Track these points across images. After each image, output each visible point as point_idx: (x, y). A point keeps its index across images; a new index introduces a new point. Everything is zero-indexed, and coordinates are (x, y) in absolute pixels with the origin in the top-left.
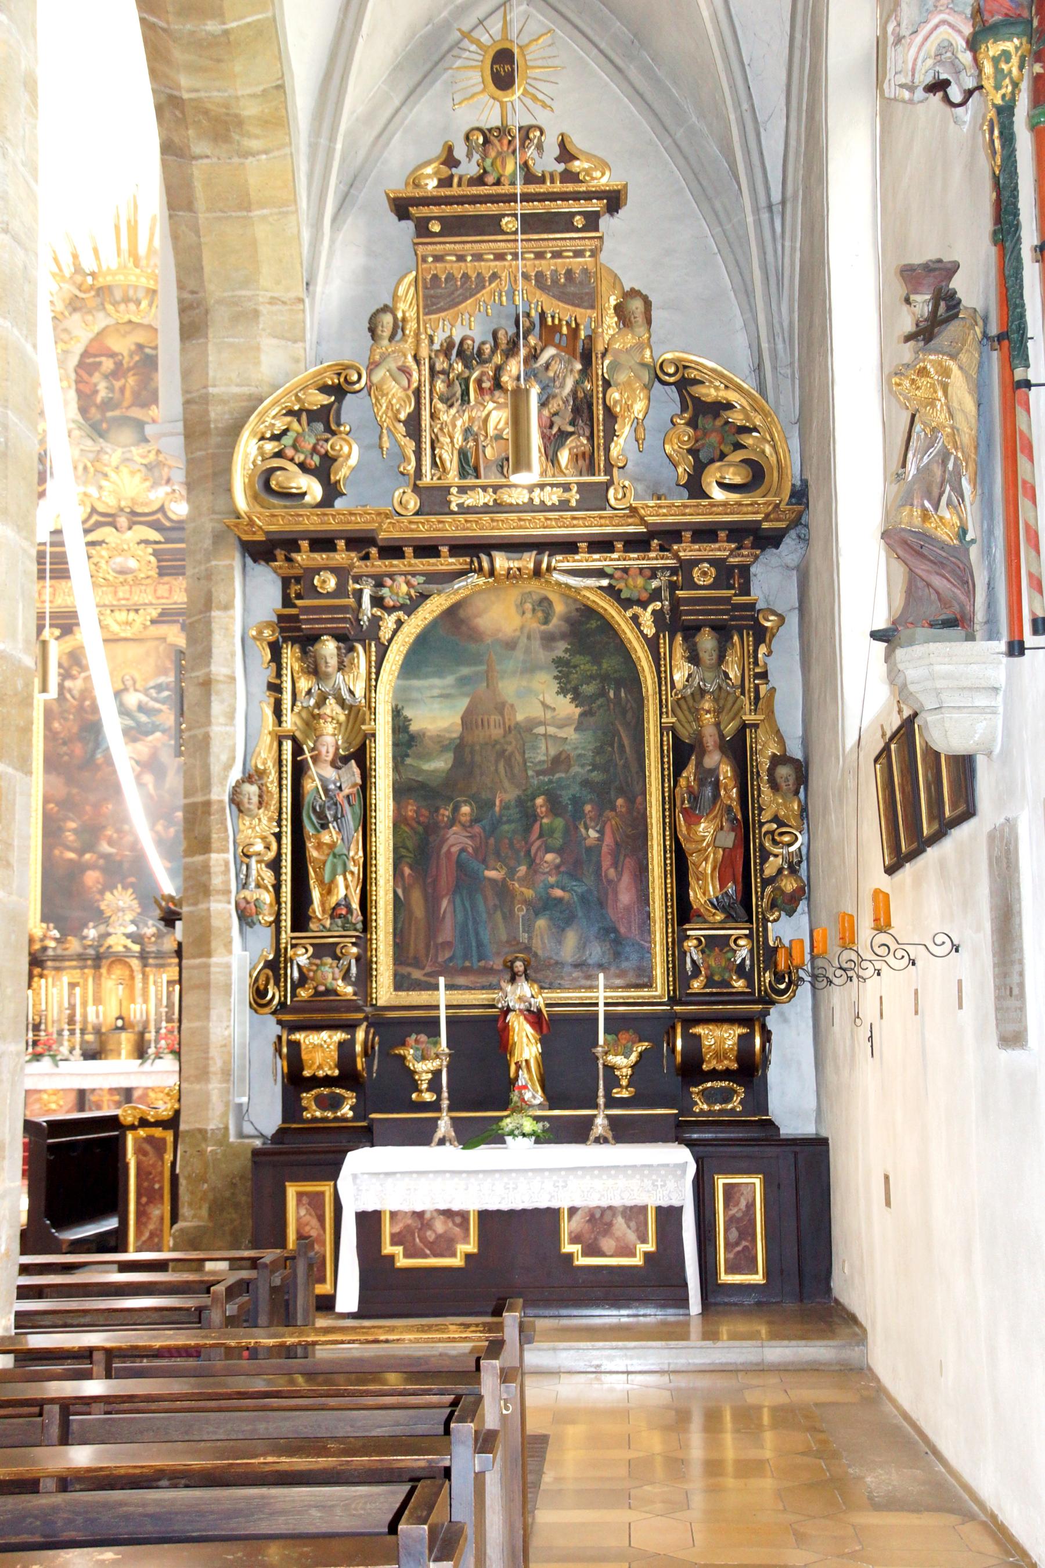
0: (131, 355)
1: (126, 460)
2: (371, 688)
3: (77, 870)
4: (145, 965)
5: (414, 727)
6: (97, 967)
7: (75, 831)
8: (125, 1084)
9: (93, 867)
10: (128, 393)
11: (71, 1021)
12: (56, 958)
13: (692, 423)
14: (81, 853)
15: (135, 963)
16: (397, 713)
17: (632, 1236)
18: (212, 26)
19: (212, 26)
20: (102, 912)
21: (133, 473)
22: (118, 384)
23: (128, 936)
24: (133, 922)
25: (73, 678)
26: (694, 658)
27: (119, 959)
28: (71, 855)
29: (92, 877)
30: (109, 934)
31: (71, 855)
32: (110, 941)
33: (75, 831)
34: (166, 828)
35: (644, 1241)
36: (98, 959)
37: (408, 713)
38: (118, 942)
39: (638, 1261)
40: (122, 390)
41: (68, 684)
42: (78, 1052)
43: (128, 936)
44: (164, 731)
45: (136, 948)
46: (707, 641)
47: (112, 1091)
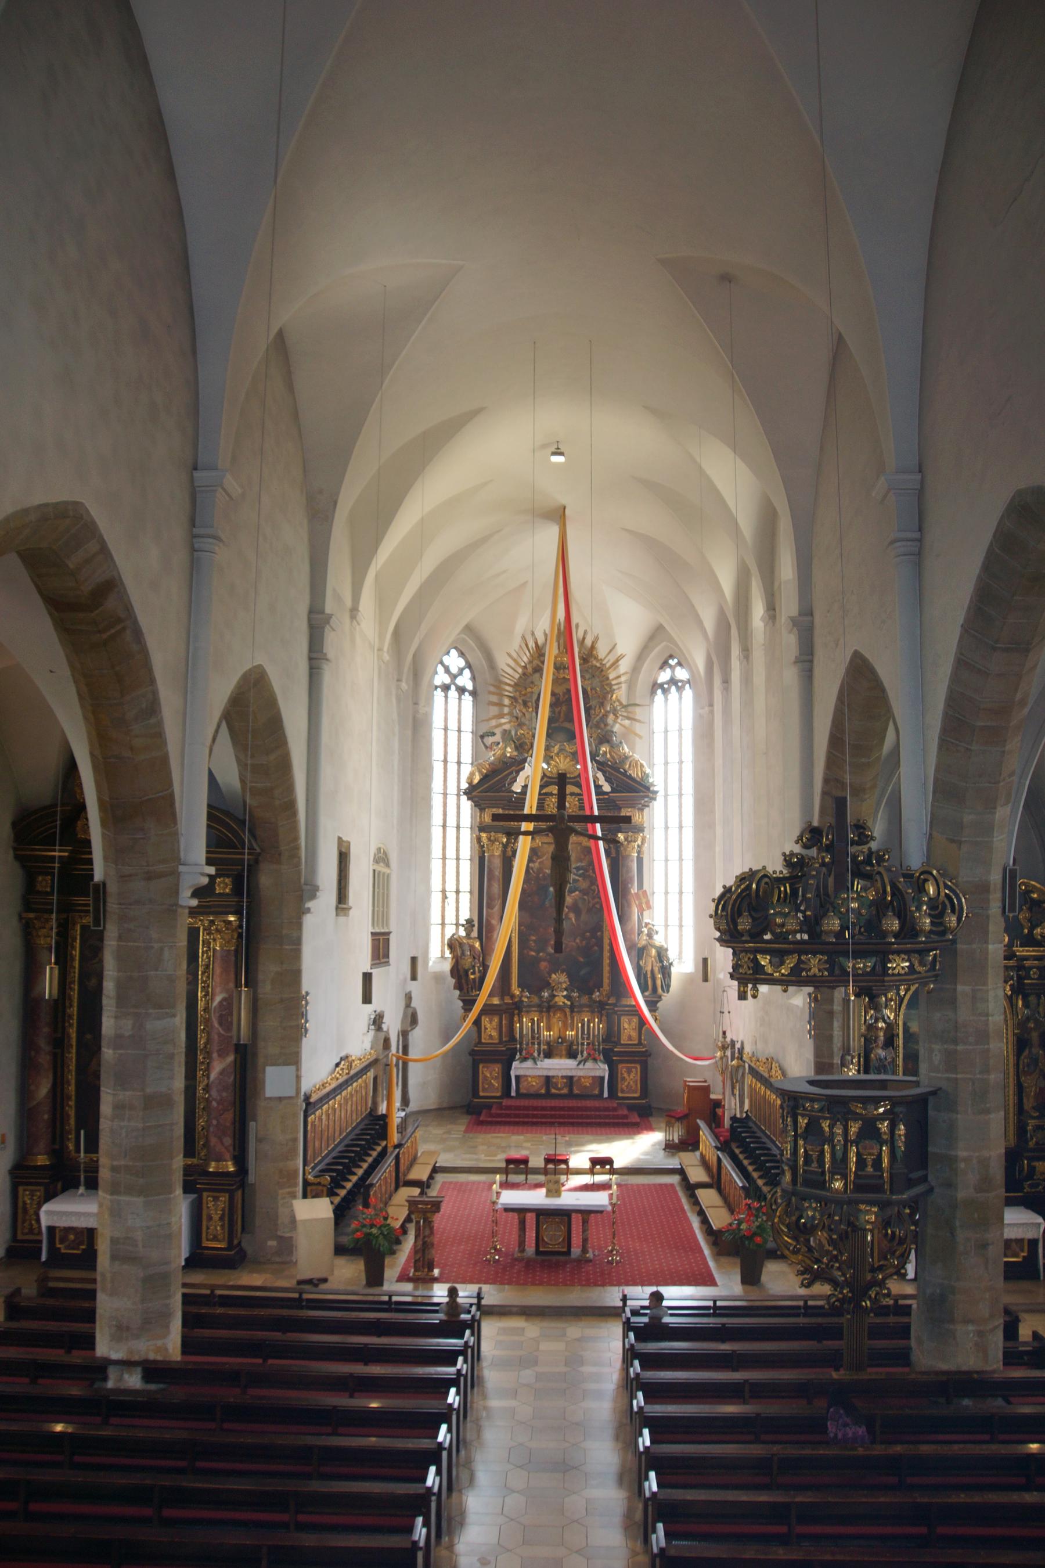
0: (564, 694)
1: (561, 750)
2: (897, 1016)
3: (537, 961)
4: (572, 1012)
5: (911, 1030)
6: (548, 1011)
7: (535, 941)
8: (570, 1074)
9: (544, 960)
10: (562, 715)
11: (533, 1038)
12: (529, 1006)
13: (1030, 909)
14: (538, 952)
15: (568, 1010)
16: (904, 1024)
17: (1018, 1250)
18: (863, 760)
19: (863, 760)
20: (549, 984)
21: (566, 757)
22: (557, 710)
23: (564, 997)
24: (566, 989)
25: (534, 862)
26: (1026, 1005)
27: (561, 1009)
28: (533, 953)
29: (543, 965)
30: (555, 996)
31: (533, 953)
32: (557, 999)
33: (535, 941)
34: (581, 941)
35: (1023, 1251)
36: (548, 1008)
37: (909, 1024)
38: (560, 1000)
39: (1020, 1259)
40: (560, 713)
41: (531, 865)
42: (542, 1055)
43: (564, 997)
44: (580, 891)
45: (569, 1003)
46: (1032, 999)
47: (563, 1077)
